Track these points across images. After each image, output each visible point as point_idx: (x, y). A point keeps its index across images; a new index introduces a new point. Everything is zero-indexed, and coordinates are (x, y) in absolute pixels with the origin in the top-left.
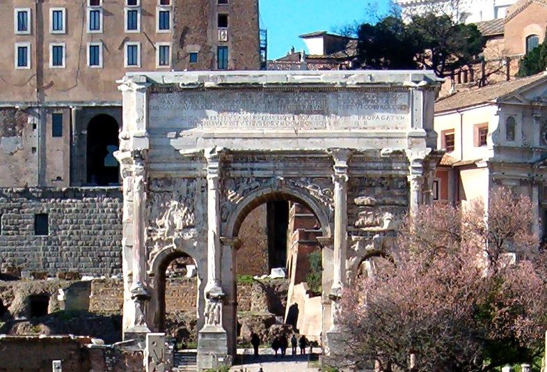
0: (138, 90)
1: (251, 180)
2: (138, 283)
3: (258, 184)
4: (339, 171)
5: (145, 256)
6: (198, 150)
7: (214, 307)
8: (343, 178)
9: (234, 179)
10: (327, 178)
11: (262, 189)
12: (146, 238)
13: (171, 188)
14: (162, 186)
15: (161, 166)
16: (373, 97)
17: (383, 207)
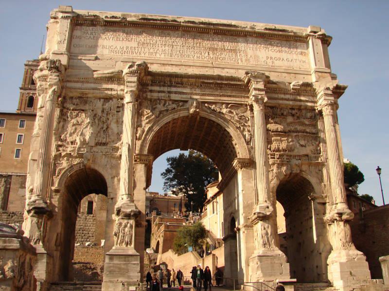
0: (62, 17)
1: (167, 104)
2: (38, 196)
3: (174, 106)
4: (257, 92)
5: (49, 167)
6: (116, 69)
7: (126, 226)
8: (262, 99)
9: (151, 100)
10: (241, 104)
11: (180, 110)
12: (53, 153)
13: (87, 107)
14: (77, 104)
15: (79, 85)
16: (278, 44)
17: (296, 134)
